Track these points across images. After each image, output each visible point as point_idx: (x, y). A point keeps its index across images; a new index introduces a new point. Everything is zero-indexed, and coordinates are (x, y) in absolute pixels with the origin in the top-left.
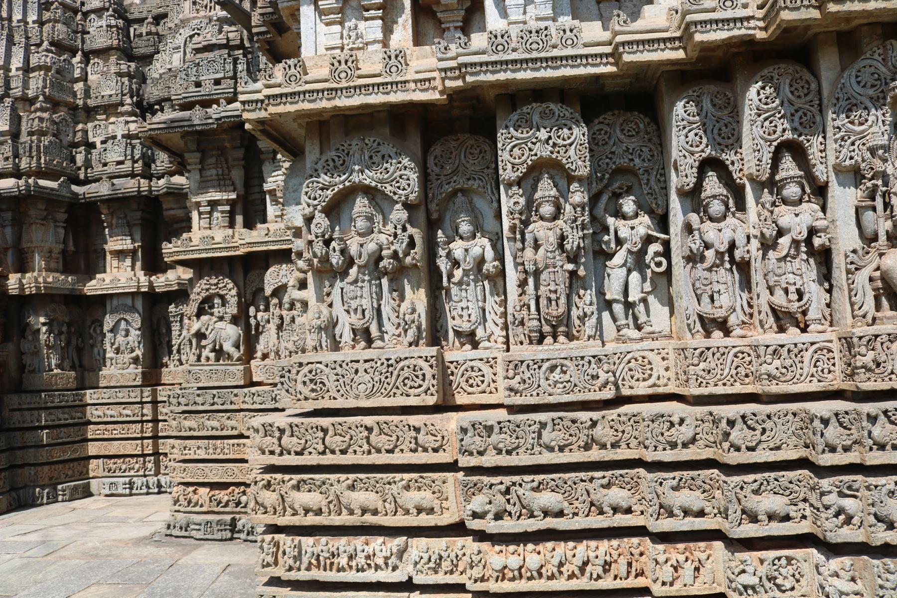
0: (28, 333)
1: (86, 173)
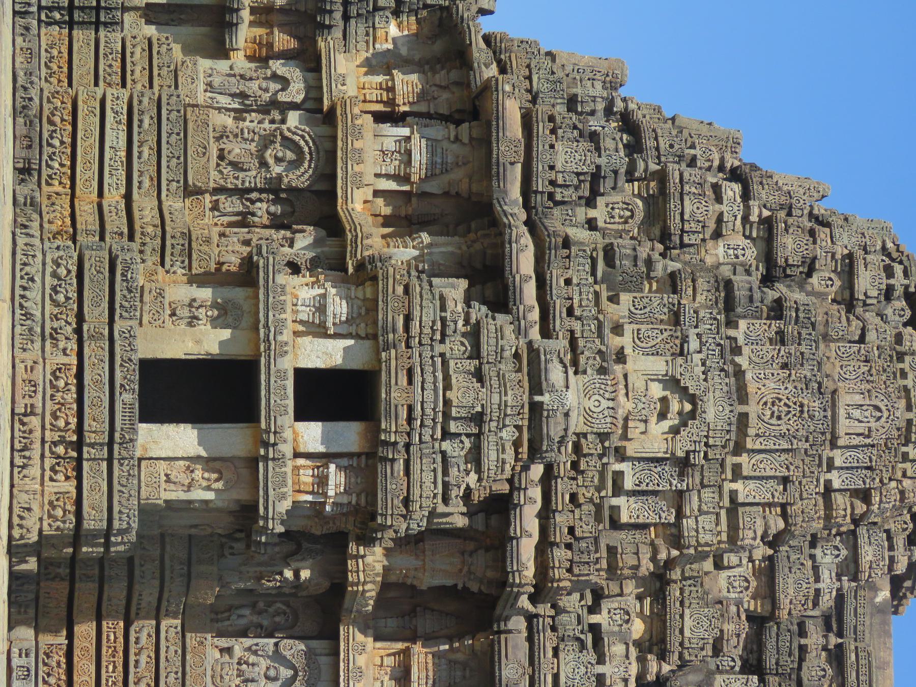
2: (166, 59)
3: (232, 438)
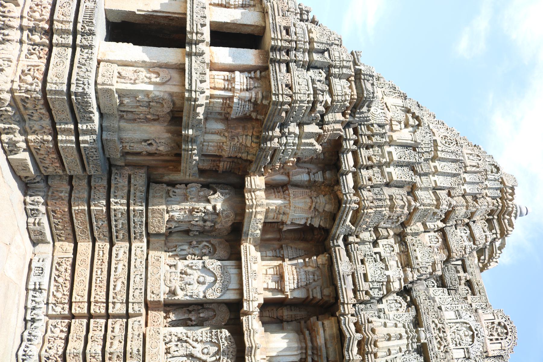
0: (206, 191)
1: (353, 243)
3: (169, 55)
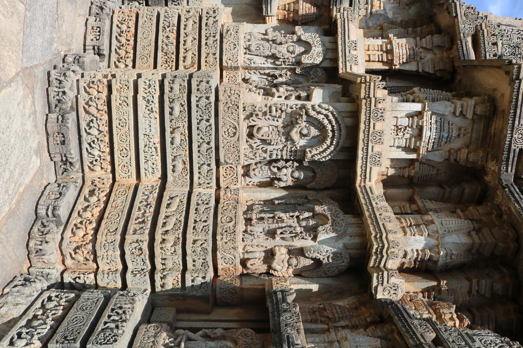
2: (212, 31)
